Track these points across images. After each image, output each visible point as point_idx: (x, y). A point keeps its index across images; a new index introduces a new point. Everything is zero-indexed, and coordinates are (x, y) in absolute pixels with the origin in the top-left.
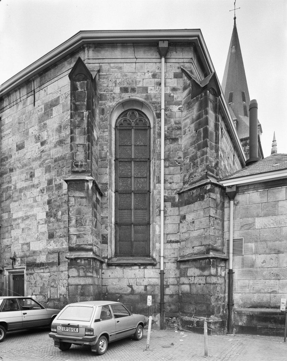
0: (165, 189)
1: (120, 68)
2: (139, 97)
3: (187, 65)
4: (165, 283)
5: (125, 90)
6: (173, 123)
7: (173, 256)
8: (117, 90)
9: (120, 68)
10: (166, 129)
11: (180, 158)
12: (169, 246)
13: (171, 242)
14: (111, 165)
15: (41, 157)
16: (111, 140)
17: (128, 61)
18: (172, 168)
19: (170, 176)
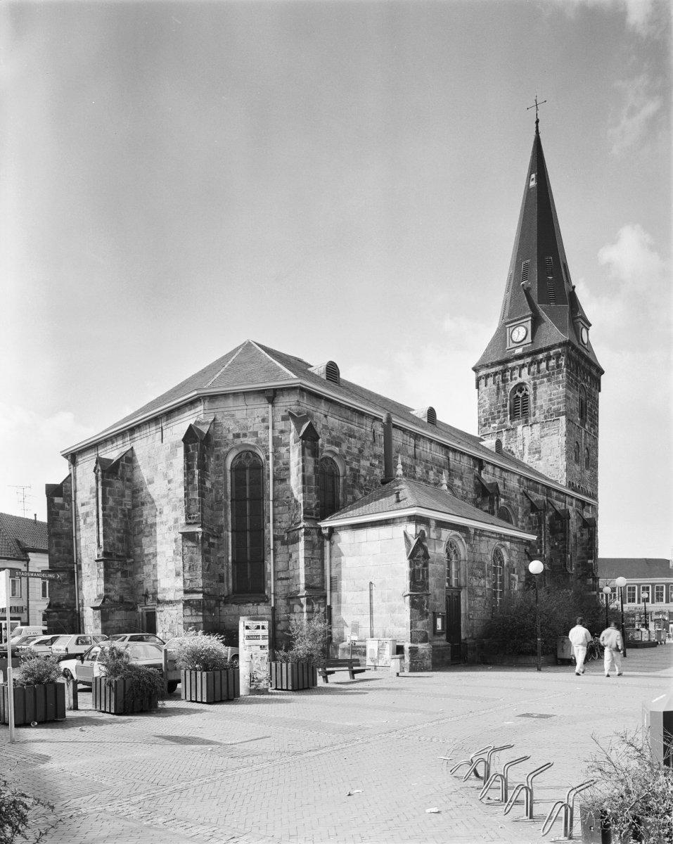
0: (274, 527)
1: (233, 415)
2: (250, 441)
3: (293, 407)
4: (276, 619)
5: (237, 436)
6: (281, 464)
7: (283, 592)
8: (230, 437)
9: (233, 415)
10: (275, 470)
11: (288, 497)
12: (279, 583)
13: (282, 579)
14: (226, 508)
15: (168, 495)
16: (226, 483)
17: (240, 408)
18: (281, 508)
19: (279, 516)
